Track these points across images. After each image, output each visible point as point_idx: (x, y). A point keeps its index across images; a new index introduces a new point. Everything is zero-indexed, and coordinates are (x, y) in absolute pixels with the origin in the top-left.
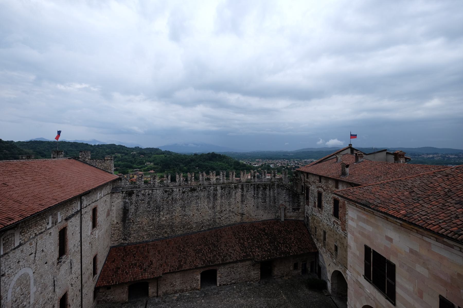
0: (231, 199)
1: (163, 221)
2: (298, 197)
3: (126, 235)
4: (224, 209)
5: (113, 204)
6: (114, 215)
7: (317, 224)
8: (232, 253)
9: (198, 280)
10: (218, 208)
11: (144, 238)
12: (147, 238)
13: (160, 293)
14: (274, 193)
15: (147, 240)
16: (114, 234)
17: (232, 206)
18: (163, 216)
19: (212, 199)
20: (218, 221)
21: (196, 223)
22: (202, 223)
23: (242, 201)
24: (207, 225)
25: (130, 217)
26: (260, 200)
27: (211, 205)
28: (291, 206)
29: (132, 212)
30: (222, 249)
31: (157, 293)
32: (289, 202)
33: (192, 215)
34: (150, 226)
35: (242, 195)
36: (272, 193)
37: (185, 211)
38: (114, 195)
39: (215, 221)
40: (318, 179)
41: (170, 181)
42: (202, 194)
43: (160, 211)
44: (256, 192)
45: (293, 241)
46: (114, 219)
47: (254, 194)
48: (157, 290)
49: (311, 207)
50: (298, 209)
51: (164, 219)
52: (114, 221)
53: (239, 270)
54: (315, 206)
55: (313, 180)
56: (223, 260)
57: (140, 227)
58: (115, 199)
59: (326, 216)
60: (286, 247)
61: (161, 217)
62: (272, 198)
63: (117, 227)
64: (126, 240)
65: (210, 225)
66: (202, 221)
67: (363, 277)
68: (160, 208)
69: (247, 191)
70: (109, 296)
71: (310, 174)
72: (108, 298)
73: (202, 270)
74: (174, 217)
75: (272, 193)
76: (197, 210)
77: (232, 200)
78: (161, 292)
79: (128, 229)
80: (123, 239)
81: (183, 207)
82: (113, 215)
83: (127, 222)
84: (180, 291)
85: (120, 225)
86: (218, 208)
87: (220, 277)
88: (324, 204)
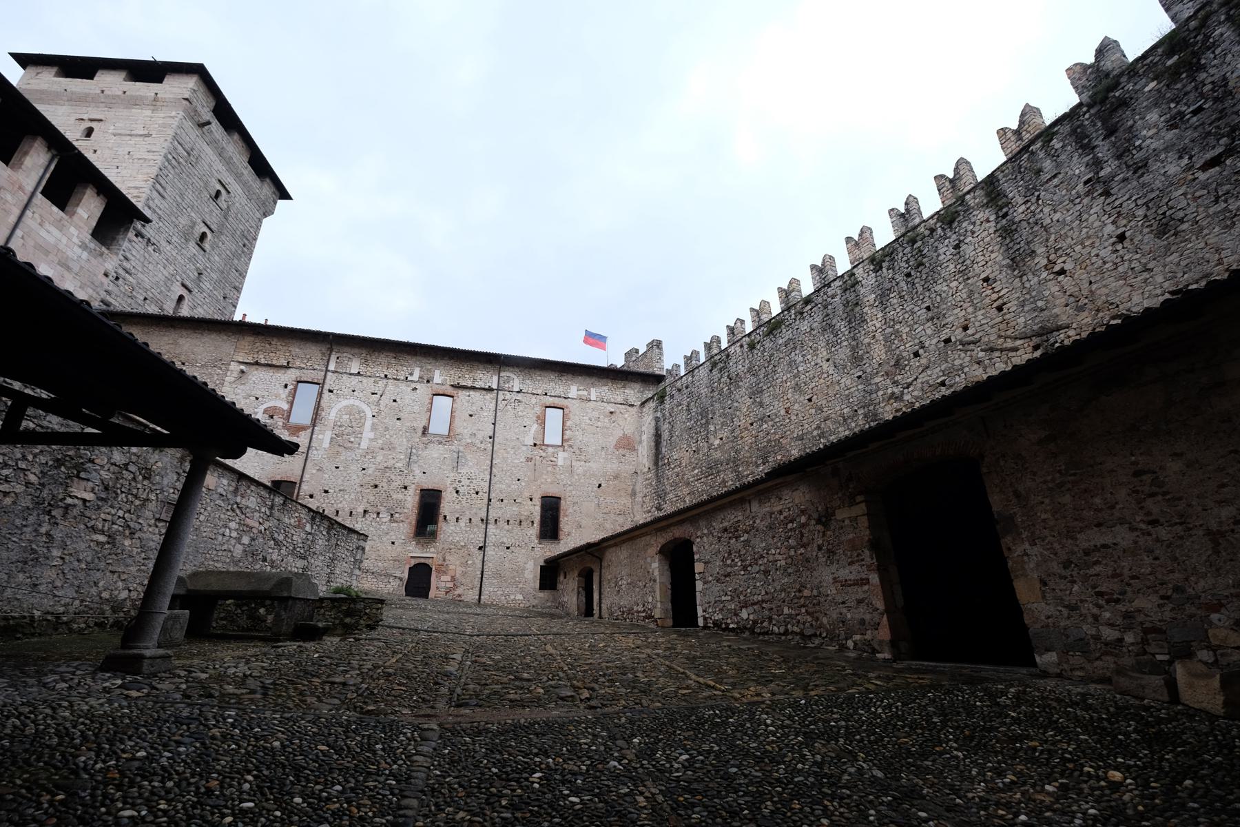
0: (941, 287)
3: (661, 495)
10: (879, 352)
17: (955, 317)
19: (842, 326)
23: (1017, 262)
27: (843, 353)
33: (783, 412)
34: (694, 468)
35: (1007, 232)
37: (761, 404)
42: (805, 326)
43: (707, 423)
44: (1103, 149)
47: (1097, 164)
66: (818, 427)
76: (797, 388)
77: (948, 287)
81: (756, 392)
86: (879, 352)
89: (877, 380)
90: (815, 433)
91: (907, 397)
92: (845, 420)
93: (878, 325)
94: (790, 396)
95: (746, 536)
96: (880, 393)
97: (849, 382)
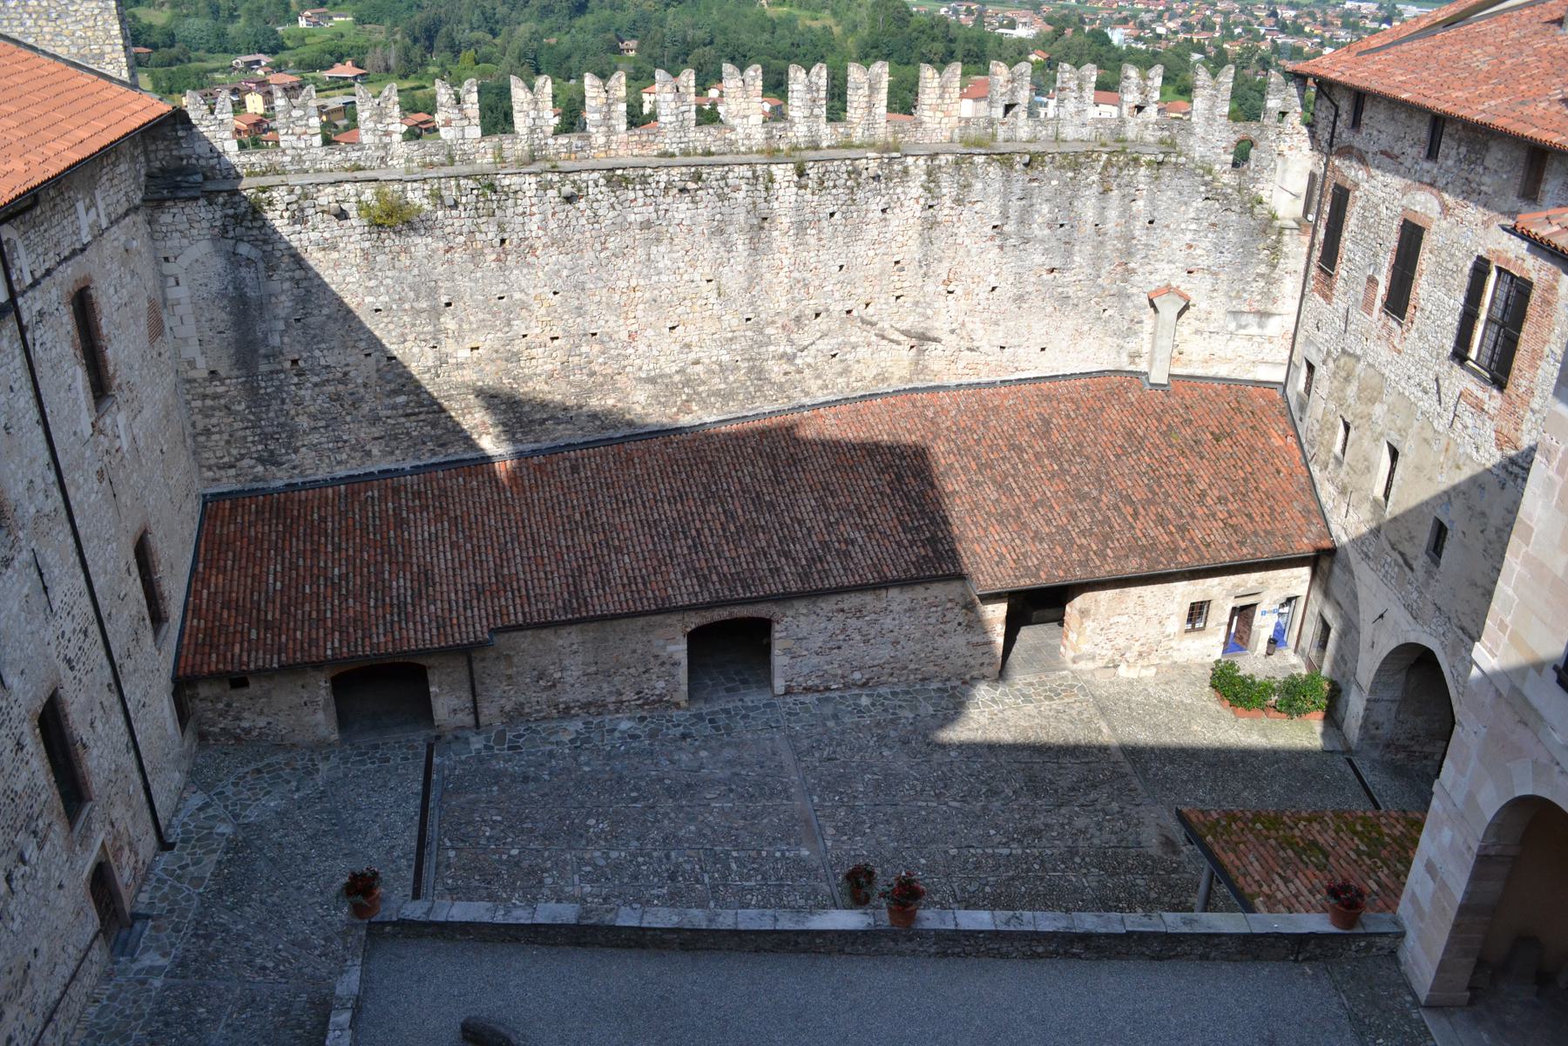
0: (860, 248)
1: (460, 366)
2: (1275, 249)
4: (809, 307)
5: (168, 268)
6: (189, 330)
7: (1360, 408)
8: (853, 542)
9: (676, 664)
11: (369, 454)
12: (385, 454)
13: (488, 712)
14: (1128, 216)
15: (385, 466)
16: (207, 432)
18: (459, 338)
19: (741, 243)
20: (775, 370)
21: (652, 380)
22: (687, 383)
24: (717, 393)
25: (275, 340)
26: (1038, 258)
28: (1220, 297)
29: (282, 313)
30: (801, 522)
31: (476, 712)
32: (1215, 274)
33: (624, 336)
34: (395, 393)
35: (932, 224)
36: (1113, 213)
37: (580, 311)
38: (166, 218)
39: (757, 373)
40: (1424, 133)
41: (477, 132)
43: (435, 313)
45: (1203, 494)
46: (192, 351)
48: (475, 701)
49: (1342, 306)
50: (1264, 315)
51: (463, 354)
52: (192, 364)
53: (888, 622)
54: (1368, 306)
55: (1385, 141)
56: (805, 576)
57: (337, 398)
58: (175, 241)
59: (1421, 363)
60: (1161, 520)
61: (448, 346)
62: (1112, 245)
63: (216, 397)
64: (279, 464)
65: (726, 396)
67: (1554, 676)
68: (433, 293)
69: (958, 201)
70: (246, 714)
71: (1378, 97)
72: (245, 724)
73: (695, 621)
74: (519, 345)
75: (1113, 213)
78: (495, 710)
79: (275, 405)
80: (260, 460)
82: (182, 332)
83: (264, 367)
84: (586, 706)
85: (231, 387)
87: (787, 651)
88: (1422, 287)
89: (769, 330)
90: (677, 378)
91: (798, 361)
92: (722, 371)
93: (786, 262)
94: (639, 314)
95: (874, 616)
96: (771, 348)
97: (735, 322)
